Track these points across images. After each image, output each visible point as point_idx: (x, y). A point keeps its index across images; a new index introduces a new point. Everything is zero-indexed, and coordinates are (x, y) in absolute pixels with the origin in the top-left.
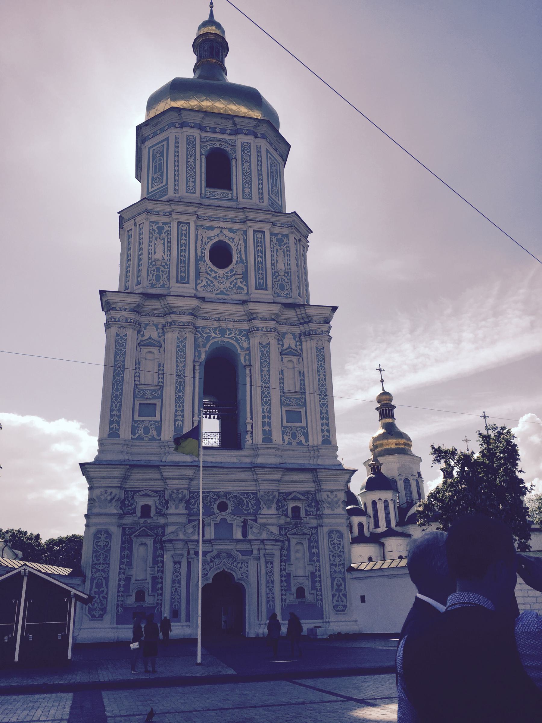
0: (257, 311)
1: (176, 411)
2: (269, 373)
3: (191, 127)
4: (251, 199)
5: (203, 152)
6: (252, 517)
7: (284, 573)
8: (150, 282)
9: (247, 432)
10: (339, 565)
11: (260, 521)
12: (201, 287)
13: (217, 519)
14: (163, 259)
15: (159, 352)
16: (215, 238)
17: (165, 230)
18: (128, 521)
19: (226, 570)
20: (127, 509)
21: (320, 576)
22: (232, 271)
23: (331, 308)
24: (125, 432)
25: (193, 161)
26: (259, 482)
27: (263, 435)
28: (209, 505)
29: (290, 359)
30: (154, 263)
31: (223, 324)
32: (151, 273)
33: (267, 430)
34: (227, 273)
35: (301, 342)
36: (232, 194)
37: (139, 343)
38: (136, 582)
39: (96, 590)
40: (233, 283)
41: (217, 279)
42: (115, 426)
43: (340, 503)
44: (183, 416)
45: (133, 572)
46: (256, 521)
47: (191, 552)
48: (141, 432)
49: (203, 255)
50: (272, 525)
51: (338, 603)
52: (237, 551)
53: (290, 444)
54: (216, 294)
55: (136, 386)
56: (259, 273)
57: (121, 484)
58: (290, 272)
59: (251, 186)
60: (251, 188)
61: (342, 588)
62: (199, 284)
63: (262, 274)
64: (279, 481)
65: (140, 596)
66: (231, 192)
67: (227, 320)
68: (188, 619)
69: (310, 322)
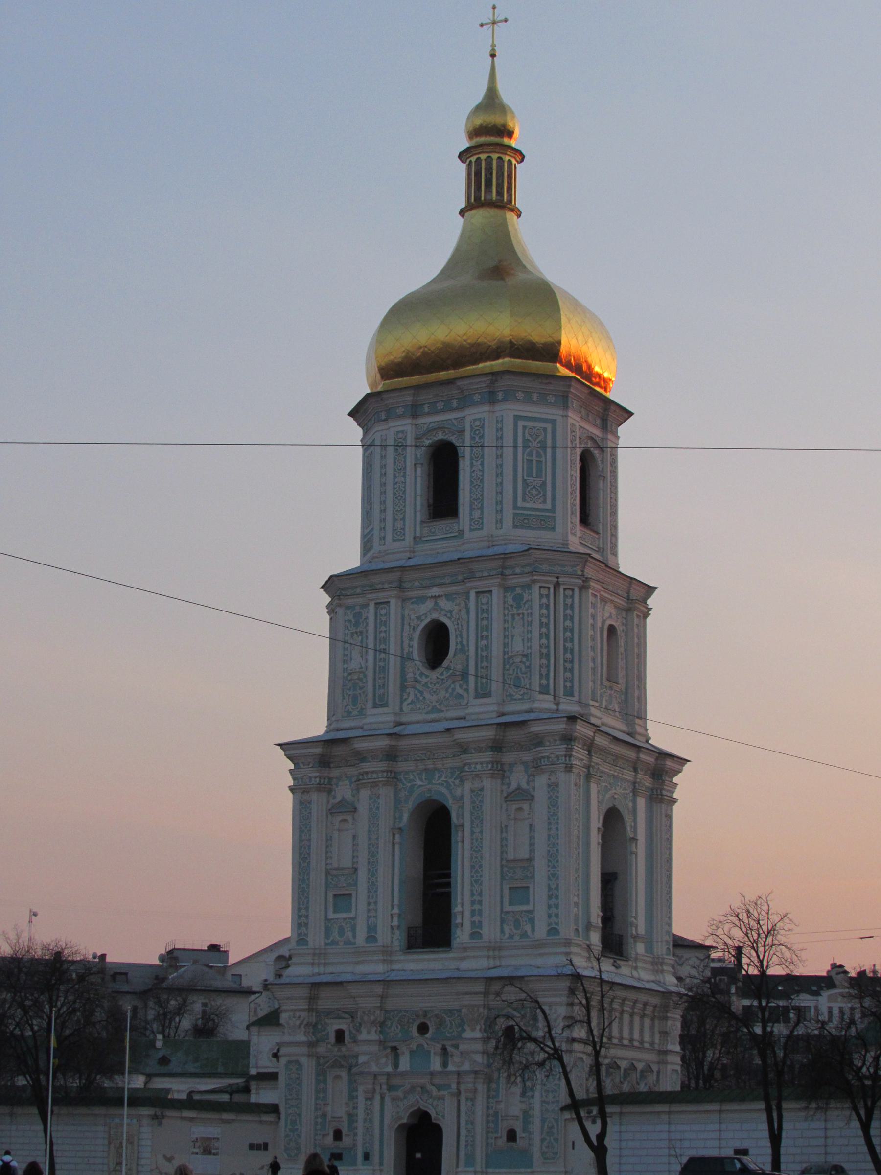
0: (467, 740)
1: (369, 904)
2: (482, 835)
3: (400, 417)
4: (482, 528)
5: (419, 456)
6: (454, 1042)
7: (491, 1112)
8: (346, 706)
9: (457, 924)
10: (553, 1102)
11: (461, 1047)
12: (408, 704)
13: (411, 1046)
14: (361, 668)
15: (354, 819)
16: (426, 617)
17: (364, 617)
18: (321, 1049)
19: (421, 1107)
20: (320, 1034)
21: (533, 1115)
22: (448, 668)
23: (565, 719)
24: (316, 938)
25: (403, 479)
26: (461, 996)
27: (472, 929)
28: (406, 1027)
29: (518, 806)
30: (349, 677)
31: (430, 765)
32: (347, 694)
33: (477, 921)
34: (442, 674)
35: (534, 776)
36: (458, 523)
37: (330, 810)
38: (332, 1119)
39: (290, 1127)
40: (450, 690)
41: (429, 688)
42: (303, 929)
43: (561, 1019)
44: (376, 911)
45: (329, 1109)
46: (456, 1047)
47: (382, 1087)
48: (335, 934)
49: (411, 649)
50: (477, 1052)
51: (546, 1150)
52: (433, 1085)
53: (511, 936)
54: (427, 713)
55: (327, 873)
56: (482, 668)
57: (309, 1005)
58: (530, 653)
59: (482, 504)
60: (482, 508)
61: (555, 1131)
62: (406, 699)
63: (487, 667)
64: (486, 994)
65: (338, 1135)
66: (456, 521)
68: (381, 1164)
69: (540, 744)
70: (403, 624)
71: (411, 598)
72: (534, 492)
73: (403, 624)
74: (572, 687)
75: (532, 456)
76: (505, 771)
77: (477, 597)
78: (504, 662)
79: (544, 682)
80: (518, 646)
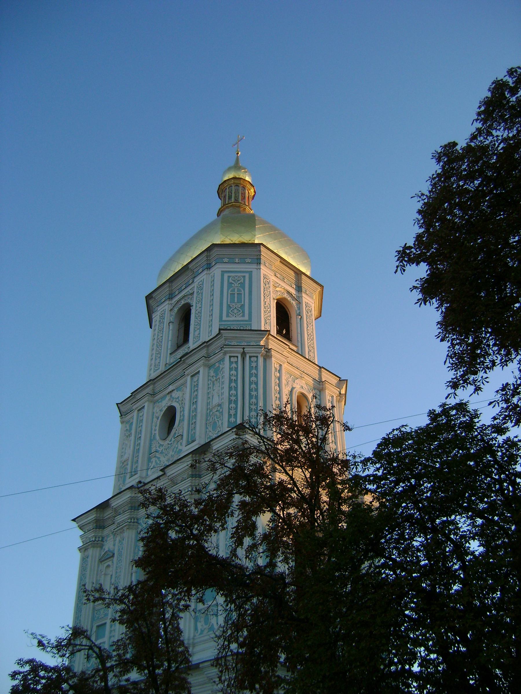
72: (235, 311)
80: (216, 401)
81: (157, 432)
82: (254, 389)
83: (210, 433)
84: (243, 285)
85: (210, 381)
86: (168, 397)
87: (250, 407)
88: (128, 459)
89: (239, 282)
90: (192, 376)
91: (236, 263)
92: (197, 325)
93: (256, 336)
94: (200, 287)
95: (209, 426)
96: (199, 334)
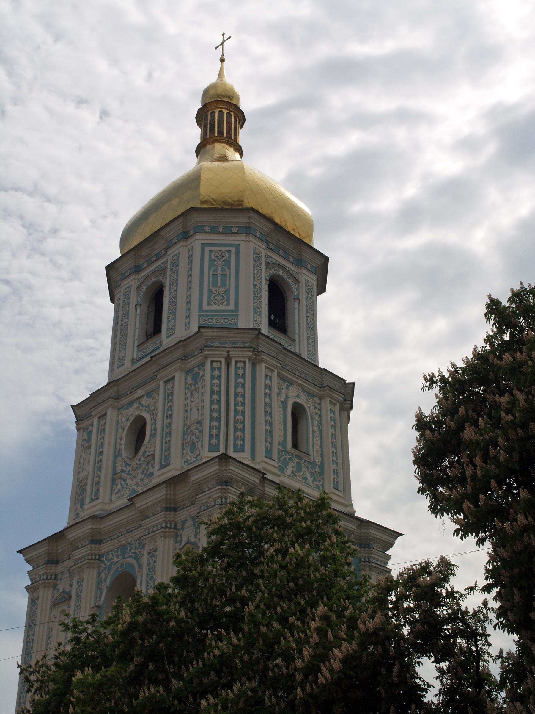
12: (116, 493)
23: (217, 460)
67: (129, 531)
70: (117, 428)
71: (123, 407)
72: (219, 298)
73: (117, 428)
74: (243, 445)
75: (218, 271)
76: (178, 530)
77: (165, 386)
78: (184, 434)
79: (214, 441)
80: (194, 416)
81: (123, 447)
82: (240, 403)
83: (188, 455)
84: (227, 263)
85: (187, 390)
86: (135, 405)
87: (235, 426)
88: (87, 478)
89: (224, 259)
90: (166, 382)
91: (219, 233)
92: (171, 313)
93: (243, 336)
94: (175, 264)
95: (186, 446)
96: (174, 326)
